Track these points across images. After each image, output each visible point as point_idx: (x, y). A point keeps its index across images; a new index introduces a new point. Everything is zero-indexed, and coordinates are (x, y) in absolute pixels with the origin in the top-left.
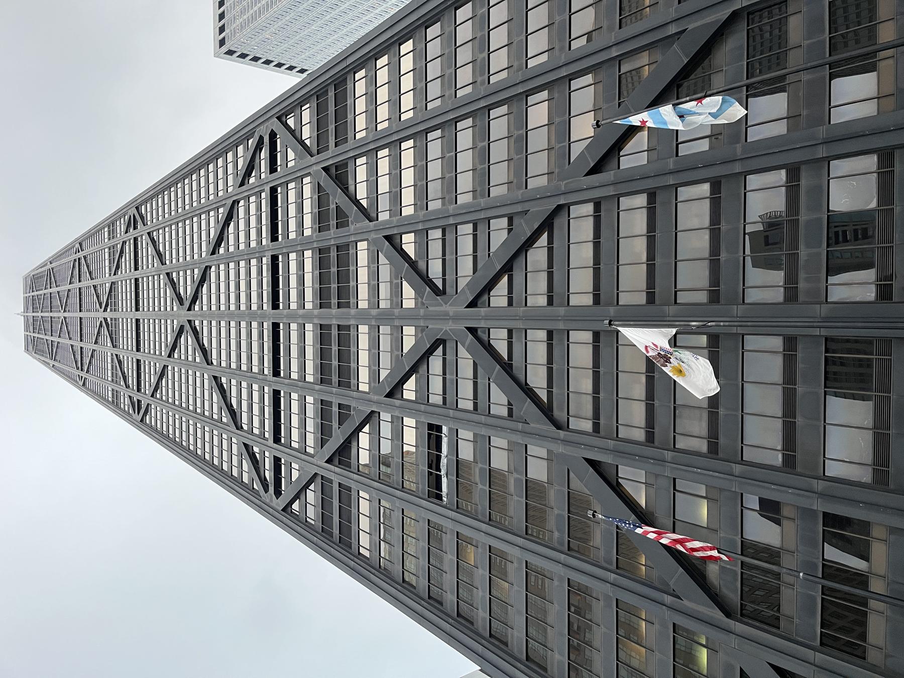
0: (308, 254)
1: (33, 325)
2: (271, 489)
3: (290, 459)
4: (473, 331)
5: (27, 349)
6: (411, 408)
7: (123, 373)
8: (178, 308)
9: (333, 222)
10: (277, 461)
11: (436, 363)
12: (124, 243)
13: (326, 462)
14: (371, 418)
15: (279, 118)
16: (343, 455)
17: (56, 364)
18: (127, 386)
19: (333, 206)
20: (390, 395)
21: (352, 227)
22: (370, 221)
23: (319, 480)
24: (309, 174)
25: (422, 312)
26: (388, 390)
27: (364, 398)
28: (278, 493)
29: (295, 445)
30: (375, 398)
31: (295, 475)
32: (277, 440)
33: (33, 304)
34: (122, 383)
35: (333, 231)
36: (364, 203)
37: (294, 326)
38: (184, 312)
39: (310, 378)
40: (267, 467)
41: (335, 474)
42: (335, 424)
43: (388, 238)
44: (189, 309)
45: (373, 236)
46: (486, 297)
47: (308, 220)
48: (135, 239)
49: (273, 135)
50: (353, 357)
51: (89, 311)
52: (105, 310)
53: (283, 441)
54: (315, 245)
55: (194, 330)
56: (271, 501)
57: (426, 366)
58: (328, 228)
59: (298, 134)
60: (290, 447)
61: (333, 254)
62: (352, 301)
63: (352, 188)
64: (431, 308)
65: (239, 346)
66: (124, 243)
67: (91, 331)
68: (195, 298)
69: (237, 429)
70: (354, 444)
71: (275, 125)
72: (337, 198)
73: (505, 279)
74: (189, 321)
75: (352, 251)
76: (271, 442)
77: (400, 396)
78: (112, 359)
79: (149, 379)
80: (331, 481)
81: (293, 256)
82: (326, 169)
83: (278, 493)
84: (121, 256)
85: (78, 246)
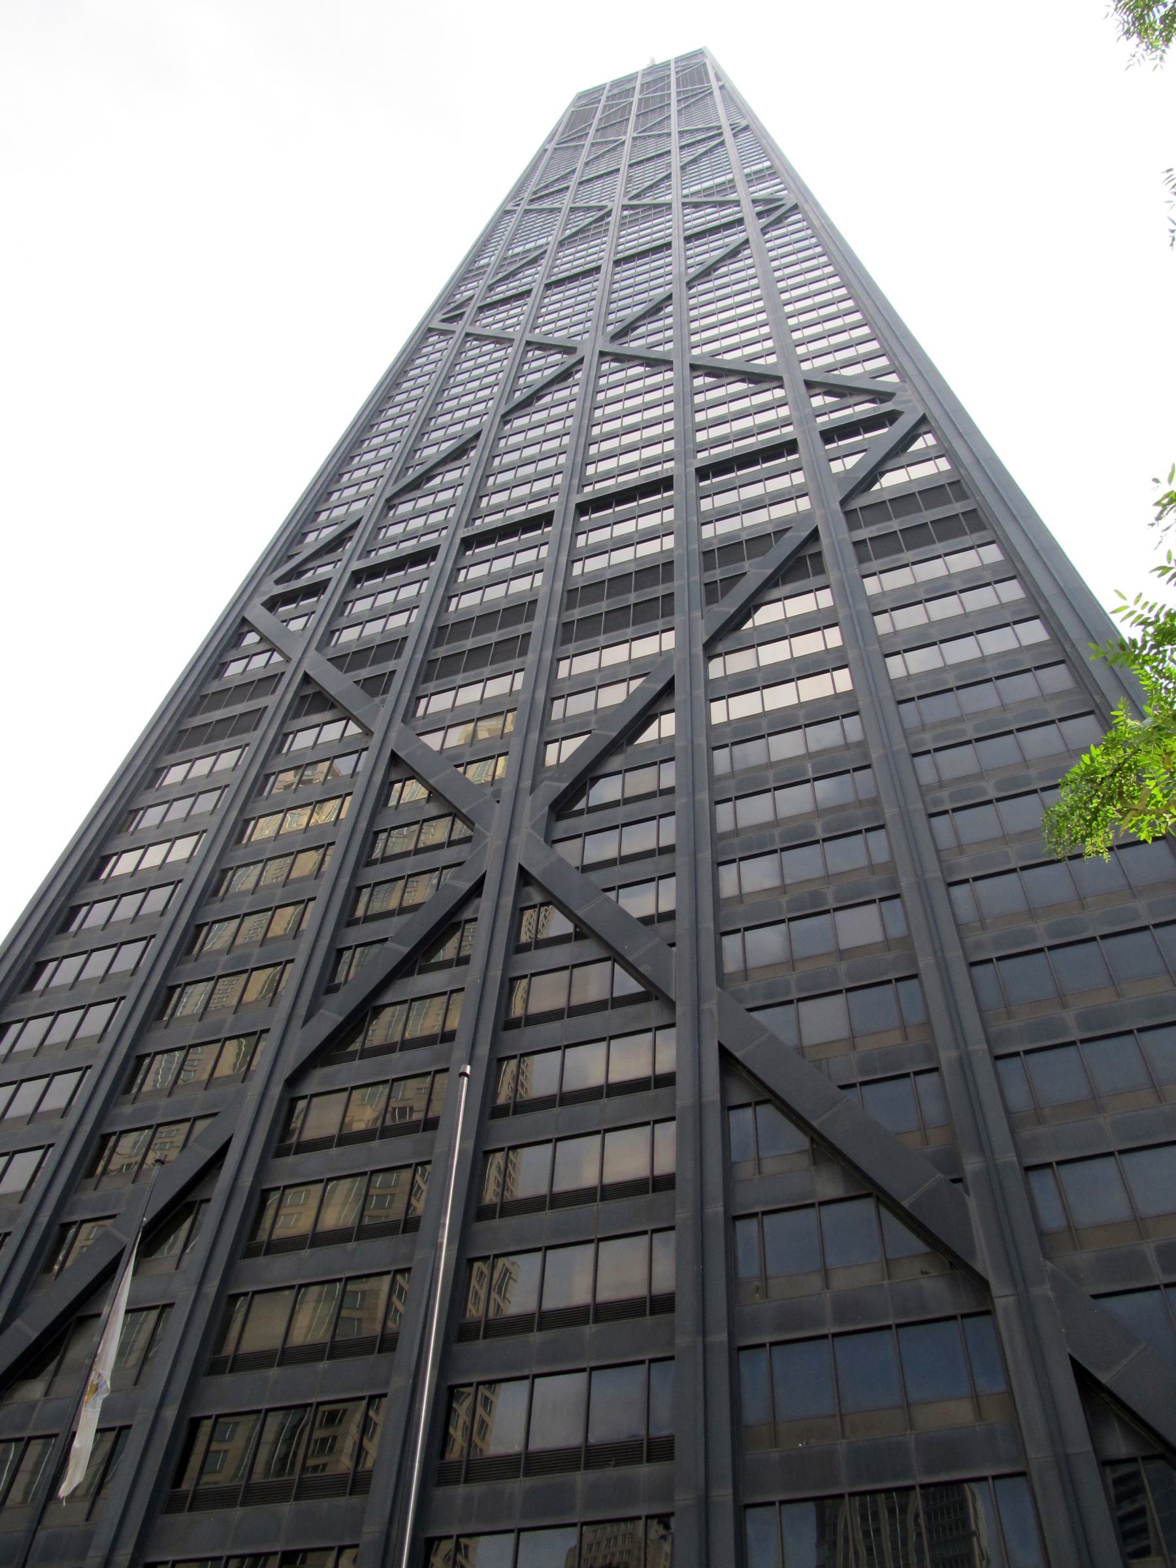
7: (513, 274)
29: (581, 541)
34: (500, 276)
37: (798, 478)
39: (707, 532)
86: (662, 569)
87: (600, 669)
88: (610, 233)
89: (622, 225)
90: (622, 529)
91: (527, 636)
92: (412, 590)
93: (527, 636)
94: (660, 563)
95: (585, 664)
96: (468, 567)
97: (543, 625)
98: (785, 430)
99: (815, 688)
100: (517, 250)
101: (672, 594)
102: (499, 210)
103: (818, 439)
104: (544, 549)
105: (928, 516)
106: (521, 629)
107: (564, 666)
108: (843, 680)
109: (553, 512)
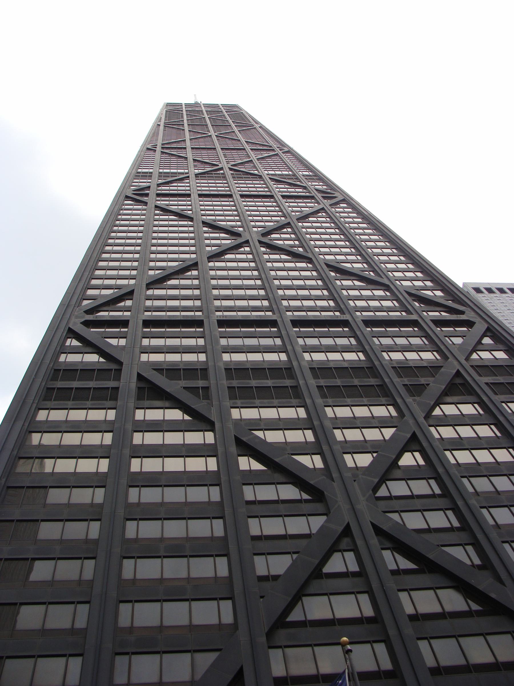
1: (194, 110)
2: (90, 317)
4: (347, 531)
5: (168, 105)
6: (228, 465)
8: (257, 232)
11: (289, 492)
12: (305, 188)
13: (139, 374)
14: (201, 421)
15: (488, 329)
16: (151, 392)
17: (162, 128)
18: (159, 185)
19: (423, 381)
20: (239, 442)
21: (409, 400)
22: (425, 418)
23: (113, 366)
24: (445, 357)
25: (349, 475)
26: (244, 439)
27: (225, 416)
28: (87, 324)
30: (231, 426)
31: (113, 342)
33: (214, 110)
34: (160, 181)
36: (437, 412)
38: (256, 238)
40: (112, 313)
41: (128, 383)
42: (183, 383)
43: (414, 437)
44: (260, 242)
45: (411, 421)
46: (388, 545)
47: (397, 356)
48: (312, 197)
49: (469, 324)
50: (266, 402)
51: (225, 156)
52: (231, 169)
55: (240, 246)
56: (77, 317)
57: (284, 480)
59: (480, 347)
61: (372, 381)
62: (330, 401)
63: (449, 399)
64: (355, 484)
65: (235, 288)
66: (305, 188)
67: (204, 156)
68: (274, 248)
70: (167, 404)
71: (480, 327)
72: (436, 385)
73: (411, 566)
74: (247, 242)
77: (240, 453)
78: (183, 173)
79: (174, 205)
82: (458, 374)
83: (87, 324)
84: (290, 184)
85: (286, 149)
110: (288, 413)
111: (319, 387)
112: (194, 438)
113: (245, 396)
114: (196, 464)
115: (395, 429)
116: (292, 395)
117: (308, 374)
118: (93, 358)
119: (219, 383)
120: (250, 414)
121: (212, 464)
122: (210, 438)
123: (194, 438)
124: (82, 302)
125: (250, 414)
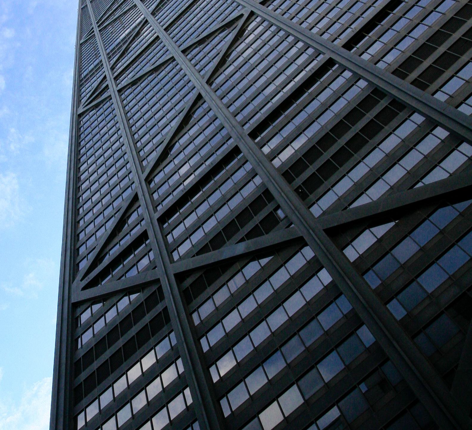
0: (362, 84)
3: (155, 246)
9: (414, 75)
10: (144, 236)
23: (154, 288)
32: (162, 220)
35: (405, 84)
53: (165, 226)
54: (376, 81)
58: (403, 76)
60: (165, 237)
61: (383, 103)
69: (146, 180)
75: (402, 115)
76: (157, 216)
80: (162, 298)
81: (347, 74)
86: (264, 196)
87: (247, 282)
88: (104, 65)
89: (109, 58)
90: (189, 222)
91: (166, 309)
92: (145, 262)
93: (166, 309)
94: (247, 205)
95: (207, 309)
96: (170, 232)
97: (171, 300)
98: (230, 142)
99: (312, 289)
100: (85, 74)
101: (166, 307)
102: (77, 46)
103: (249, 139)
104: (151, 254)
105: (327, 155)
106: (159, 308)
107: (195, 316)
108: (325, 277)
109: (146, 230)
110: (407, 129)
111: (415, 83)
112: (297, 263)
113: (308, 191)
114: (312, 289)
115: (180, 358)
116: (397, 109)
117: (396, 80)
118: (124, 303)
119: (284, 193)
120: (327, 201)
121: (325, 277)
122: (308, 253)
123: (297, 263)
124: (153, 197)
125: (327, 201)
